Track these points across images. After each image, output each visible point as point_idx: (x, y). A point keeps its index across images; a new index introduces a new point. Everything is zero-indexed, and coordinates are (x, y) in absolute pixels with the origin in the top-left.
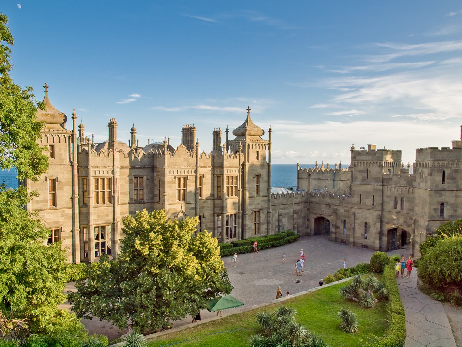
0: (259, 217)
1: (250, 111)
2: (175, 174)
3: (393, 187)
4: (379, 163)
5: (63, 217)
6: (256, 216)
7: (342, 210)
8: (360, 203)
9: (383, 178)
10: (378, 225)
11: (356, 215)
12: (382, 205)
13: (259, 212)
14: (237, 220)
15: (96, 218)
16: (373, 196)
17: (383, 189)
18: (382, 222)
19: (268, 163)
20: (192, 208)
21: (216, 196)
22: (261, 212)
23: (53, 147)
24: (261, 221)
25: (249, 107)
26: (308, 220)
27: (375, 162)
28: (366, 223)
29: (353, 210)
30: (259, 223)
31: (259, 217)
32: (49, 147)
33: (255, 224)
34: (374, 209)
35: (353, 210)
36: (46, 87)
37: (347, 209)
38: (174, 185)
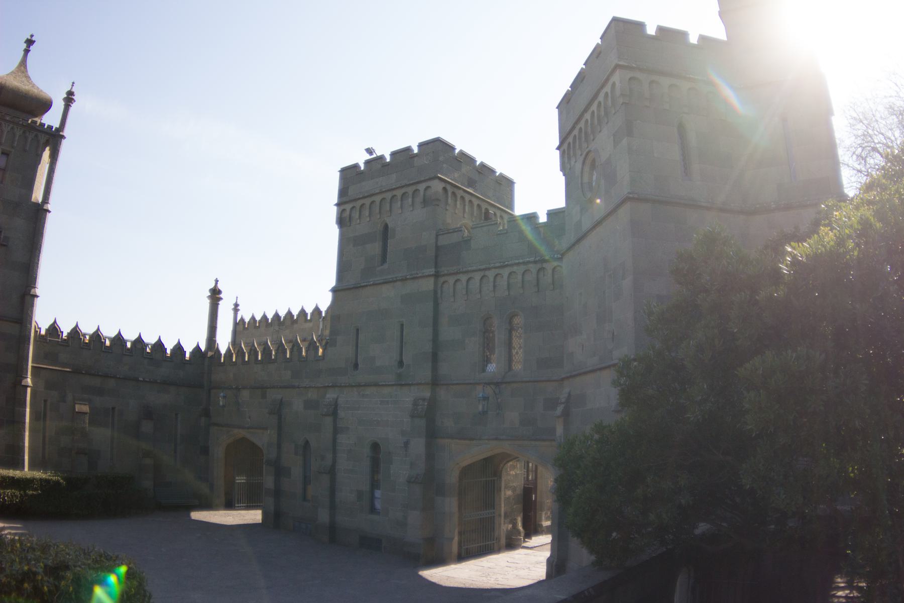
3: (477, 276)
4: (422, 193)
7: (298, 405)
8: (356, 366)
9: (438, 248)
10: (418, 446)
11: (341, 414)
12: (435, 357)
16: (402, 325)
17: (435, 292)
18: (432, 434)
26: (205, 451)
27: (410, 190)
28: (375, 447)
29: (331, 395)
34: (401, 383)
35: (331, 395)
37: (312, 395)
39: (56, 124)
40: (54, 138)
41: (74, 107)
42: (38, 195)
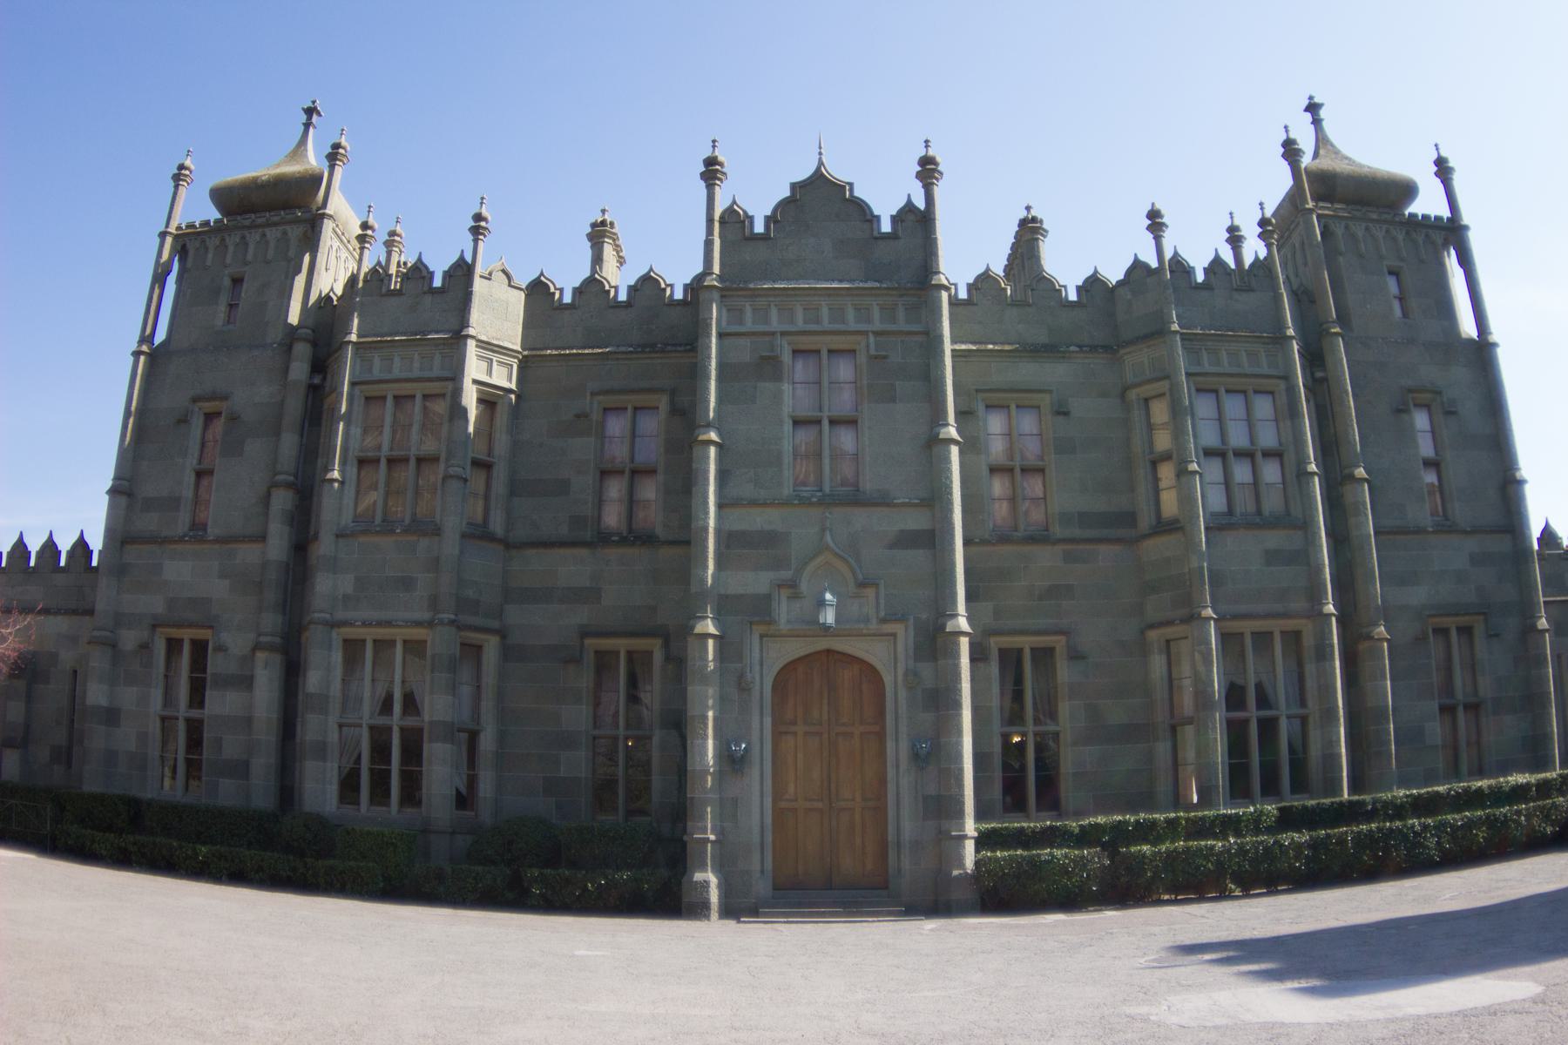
0: (1472, 667)
1: (1323, 113)
2: (775, 324)
5: (227, 582)
6: (1449, 658)
13: (1466, 631)
14: (1310, 669)
15: (349, 590)
19: (1474, 334)
20: (908, 540)
21: (1145, 521)
22: (1479, 632)
23: (237, 281)
24: (1486, 688)
25: (1311, 98)
30: (1474, 708)
31: (1472, 667)
32: (227, 282)
33: (1448, 710)
36: (310, 111)
38: (769, 385)
39: (1445, 213)
40: (1451, 232)
41: (1458, 182)
42: (1468, 328)
